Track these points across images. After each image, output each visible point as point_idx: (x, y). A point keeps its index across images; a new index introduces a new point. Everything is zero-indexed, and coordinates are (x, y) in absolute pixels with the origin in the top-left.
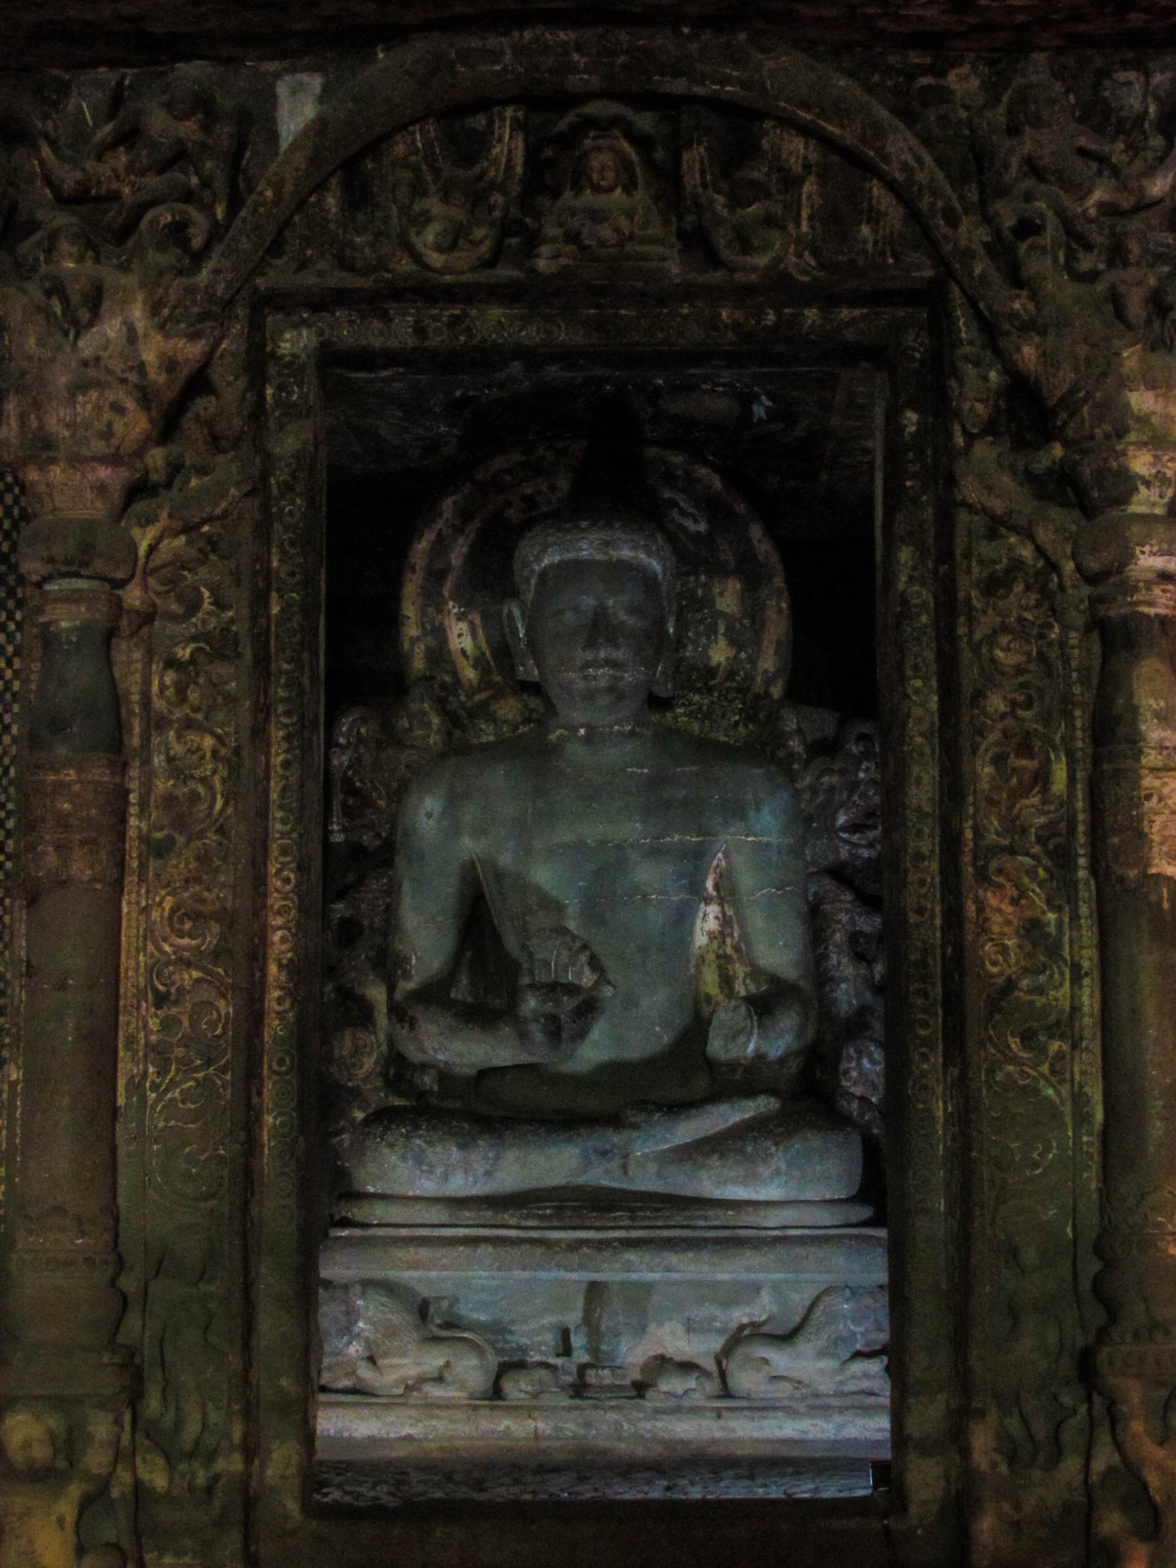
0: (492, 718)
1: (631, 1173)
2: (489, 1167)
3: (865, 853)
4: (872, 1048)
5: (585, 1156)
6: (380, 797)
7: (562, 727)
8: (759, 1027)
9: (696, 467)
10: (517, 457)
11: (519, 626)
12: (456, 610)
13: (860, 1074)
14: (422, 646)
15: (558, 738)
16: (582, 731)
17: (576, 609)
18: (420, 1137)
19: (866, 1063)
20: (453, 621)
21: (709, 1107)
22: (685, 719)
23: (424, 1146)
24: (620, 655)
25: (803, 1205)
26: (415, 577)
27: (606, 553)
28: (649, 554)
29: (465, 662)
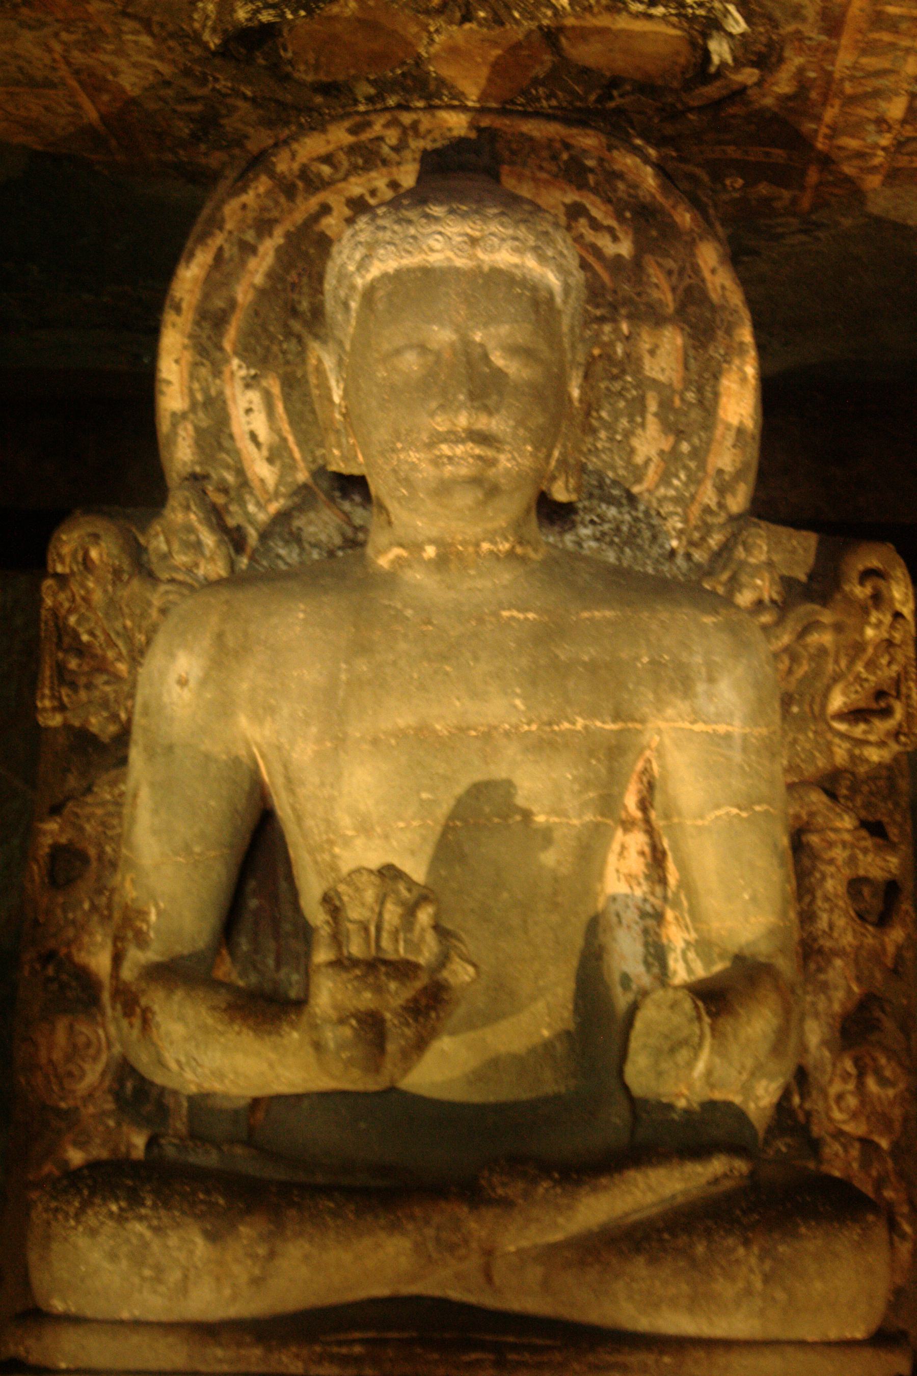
0: (296, 538)
1: (497, 1280)
2: (257, 1271)
3: (874, 755)
4: (883, 1061)
5: (418, 1248)
6: (120, 658)
7: (401, 545)
8: (713, 1036)
9: (615, 153)
10: (339, 136)
11: (333, 383)
12: (243, 373)
13: (863, 1103)
14: (190, 427)
15: (393, 562)
16: (430, 551)
17: (423, 348)
18: (141, 1218)
19: (872, 1084)
20: (238, 385)
21: (631, 1174)
22: (593, 544)
23: (148, 1234)
24: (496, 424)
25: (790, 1350)
26: (179, 320)
27: (470, 258)
28: (542, 259)
29: (252, 448)
